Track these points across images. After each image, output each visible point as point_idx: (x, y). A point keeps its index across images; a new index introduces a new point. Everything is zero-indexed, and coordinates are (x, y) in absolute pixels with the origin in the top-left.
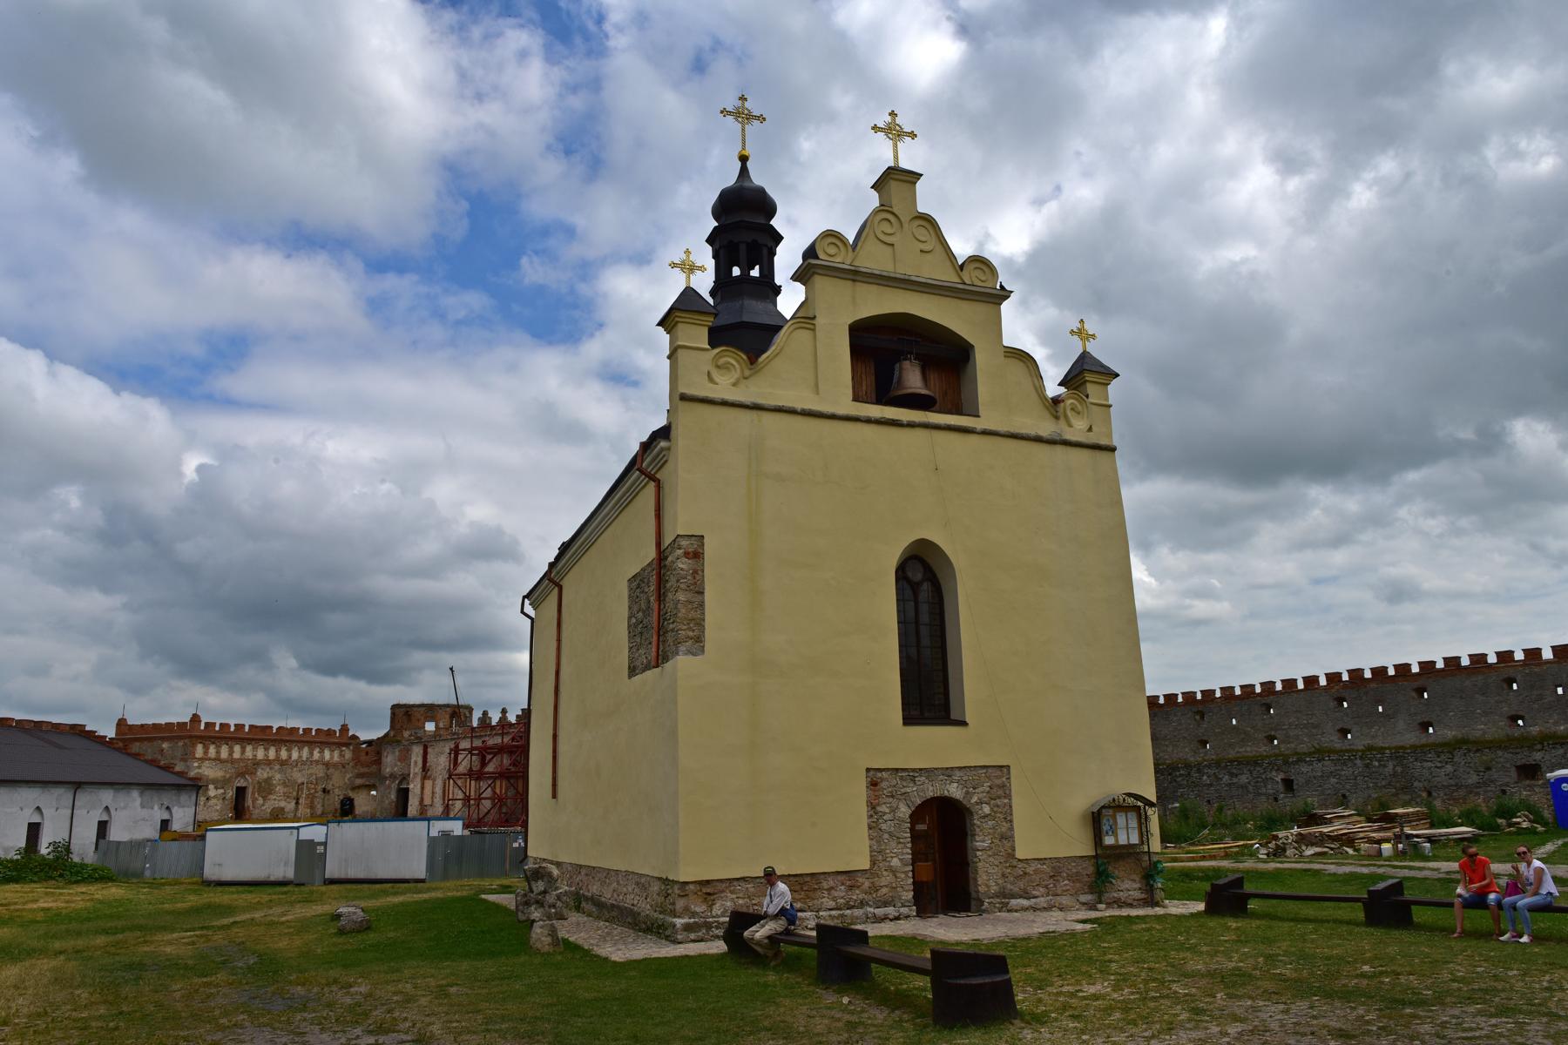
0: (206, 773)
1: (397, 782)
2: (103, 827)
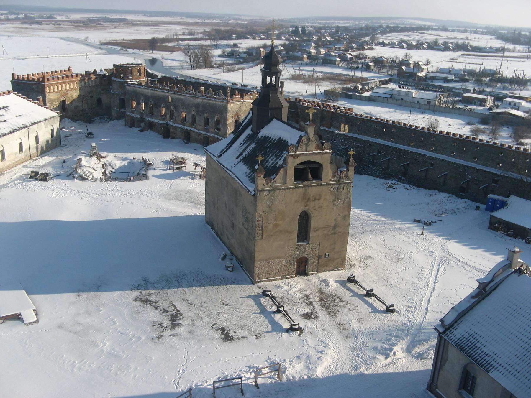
0: (51, 98)
1: (119, 96)
2: (37, 137)
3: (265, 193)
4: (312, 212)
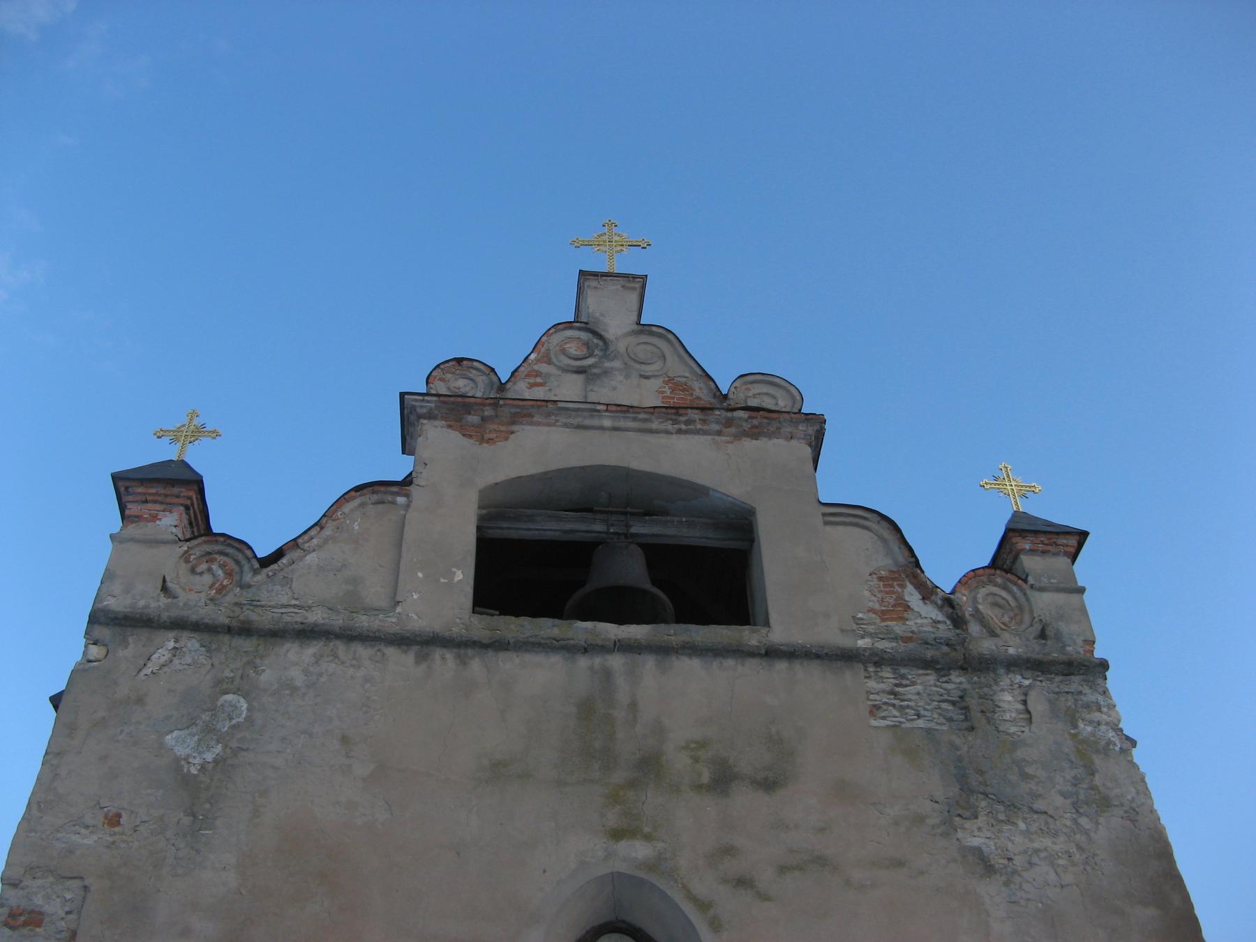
3: (161, 656)
4: (703, 906)
